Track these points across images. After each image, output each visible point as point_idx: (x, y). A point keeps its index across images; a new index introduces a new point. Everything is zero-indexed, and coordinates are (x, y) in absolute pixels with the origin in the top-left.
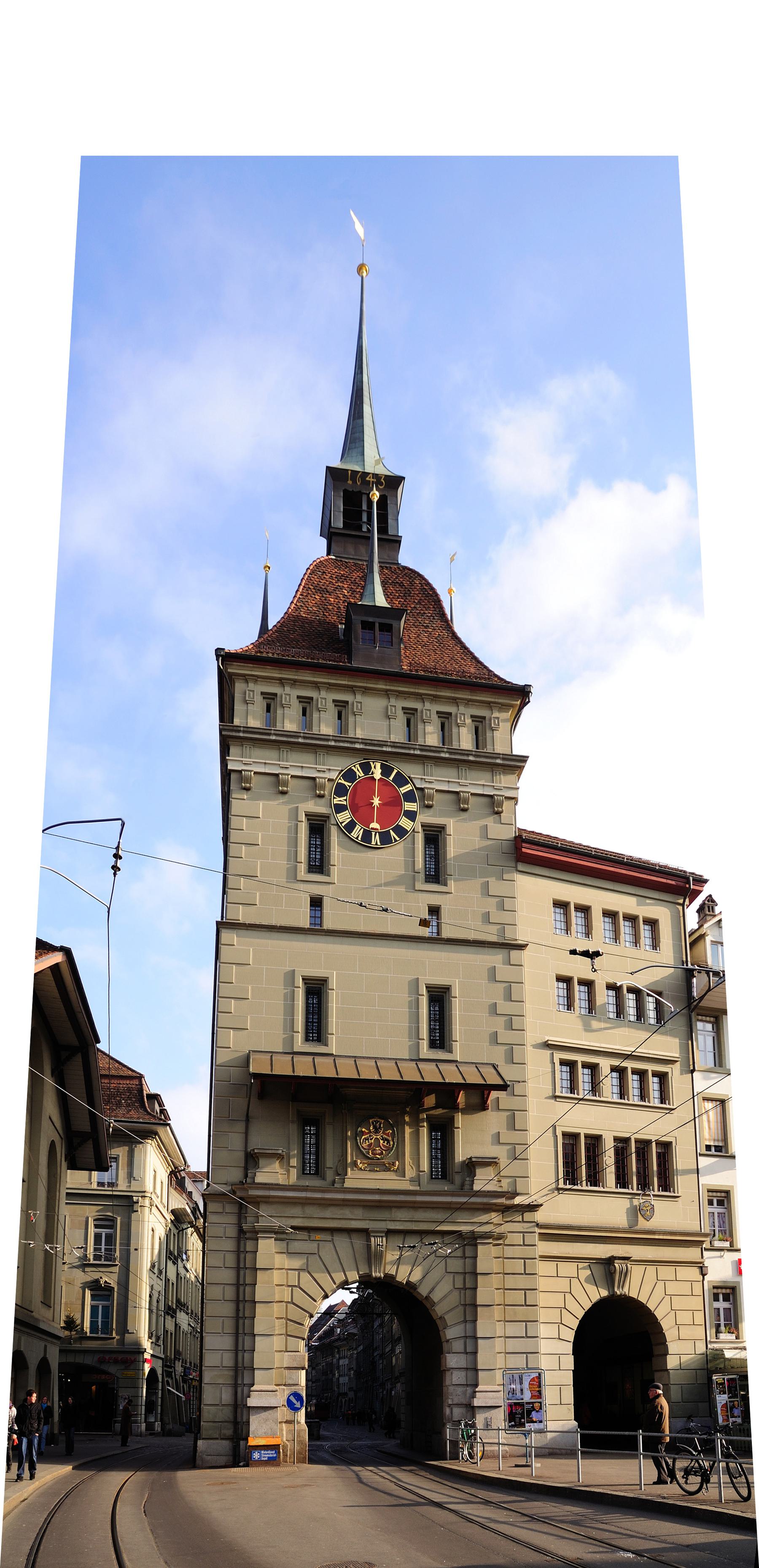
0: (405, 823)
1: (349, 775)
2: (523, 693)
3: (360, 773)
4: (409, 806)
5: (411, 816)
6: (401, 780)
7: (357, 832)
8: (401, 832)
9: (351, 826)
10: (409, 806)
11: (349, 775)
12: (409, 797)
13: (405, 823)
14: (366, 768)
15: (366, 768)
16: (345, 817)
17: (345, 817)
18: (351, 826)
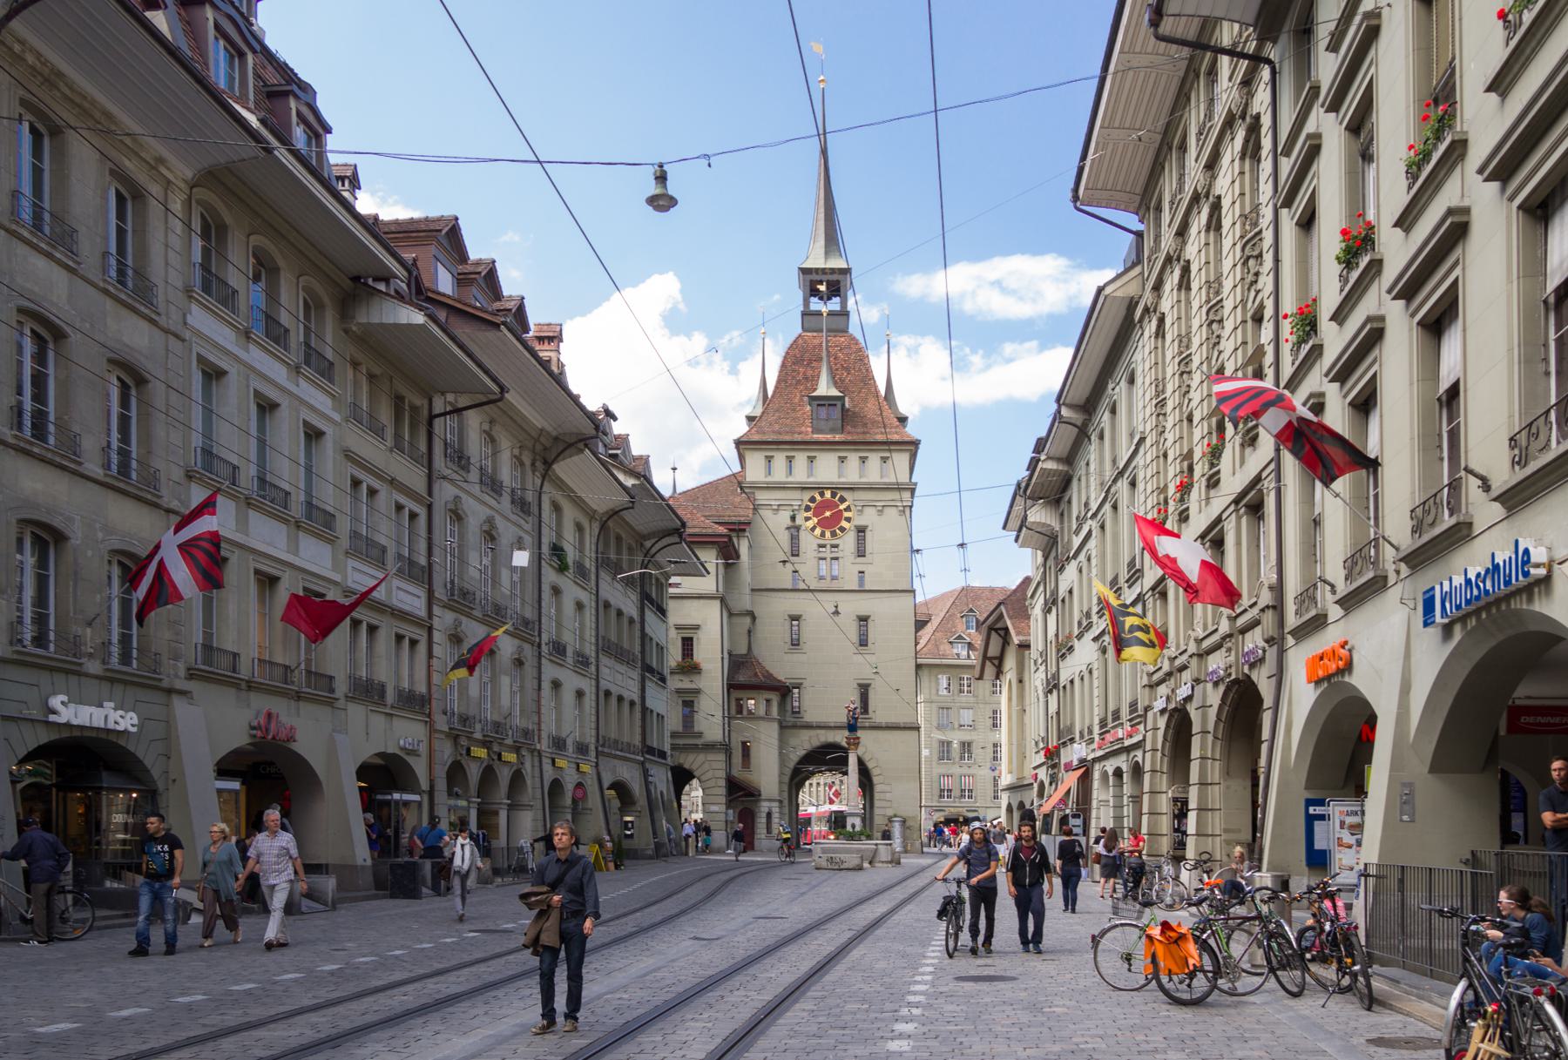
0: (844, 524)
1: (813, 500)
2: (915, 444)
3: (818, 498)
4: (846, 514)
5: (848, 520)
6: (843, 500)
7: (818, 531)
8: (843, 529)
9: (813, 529)
10: (846, 514)
11: (813, 500)
12: (848, 509)
13: (844, 524)
14: (822, 494)
15: (822, 494)
16: (810, 524)
17: (810, 524)
18: (813, 529)
